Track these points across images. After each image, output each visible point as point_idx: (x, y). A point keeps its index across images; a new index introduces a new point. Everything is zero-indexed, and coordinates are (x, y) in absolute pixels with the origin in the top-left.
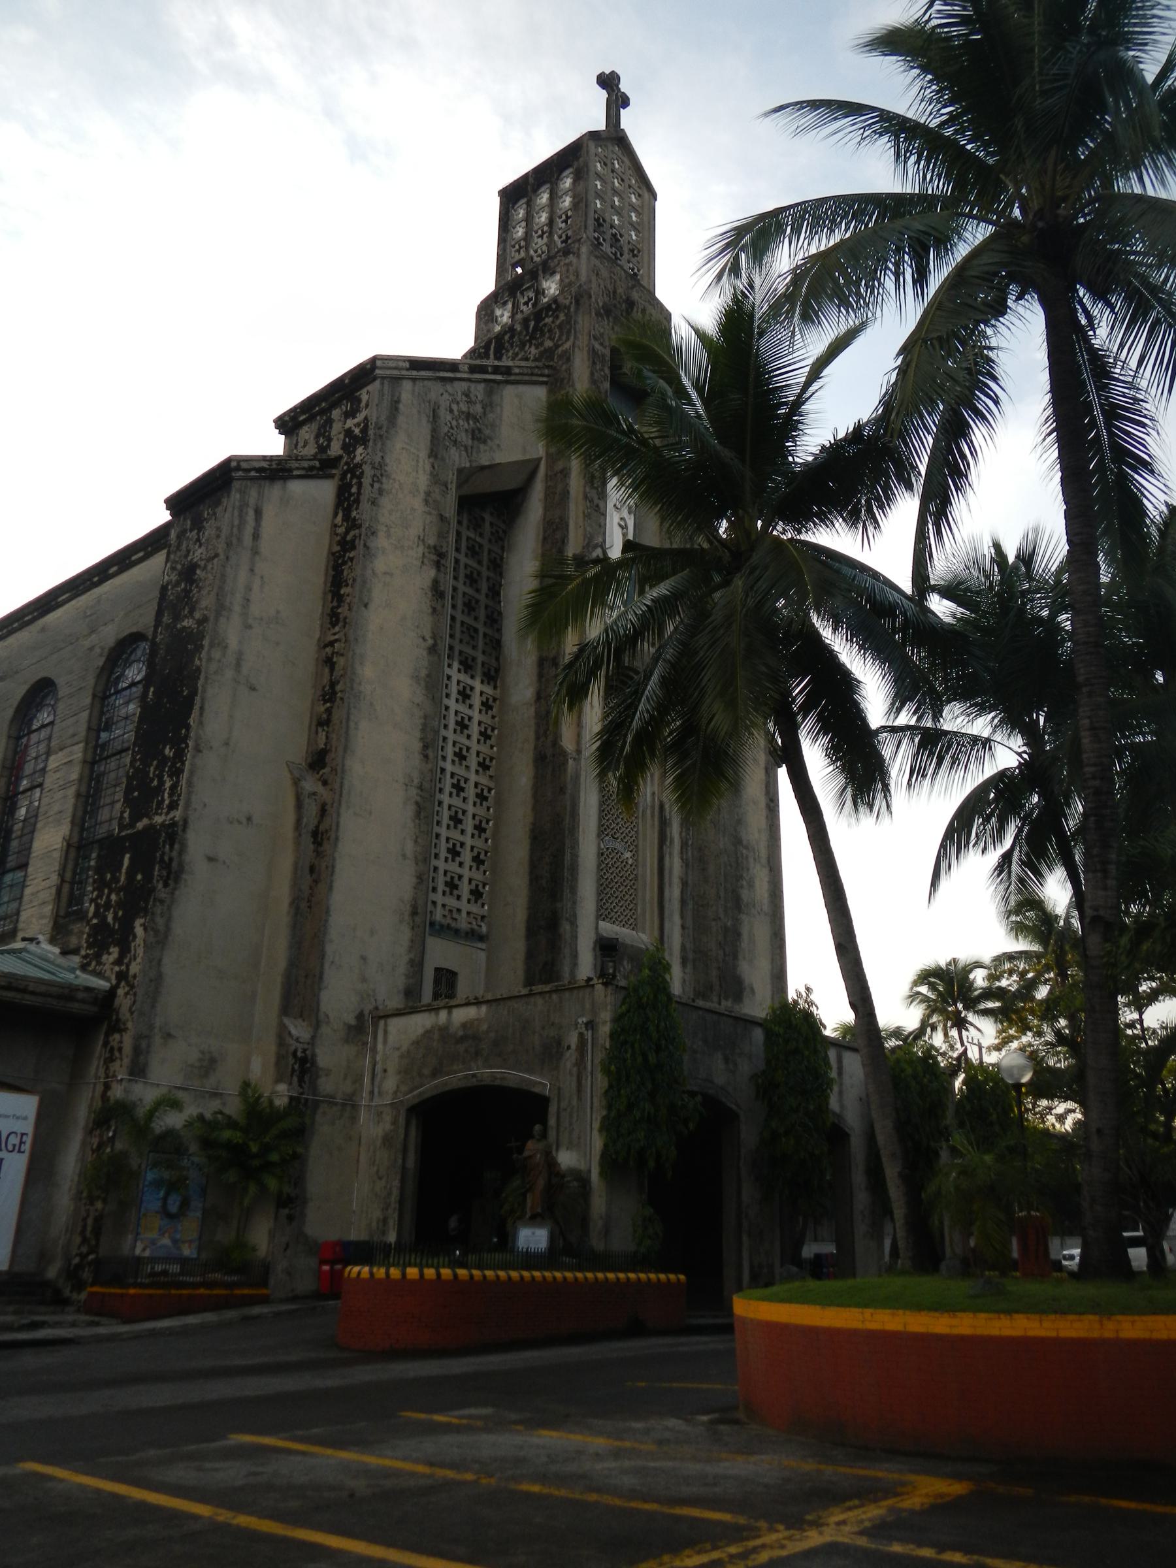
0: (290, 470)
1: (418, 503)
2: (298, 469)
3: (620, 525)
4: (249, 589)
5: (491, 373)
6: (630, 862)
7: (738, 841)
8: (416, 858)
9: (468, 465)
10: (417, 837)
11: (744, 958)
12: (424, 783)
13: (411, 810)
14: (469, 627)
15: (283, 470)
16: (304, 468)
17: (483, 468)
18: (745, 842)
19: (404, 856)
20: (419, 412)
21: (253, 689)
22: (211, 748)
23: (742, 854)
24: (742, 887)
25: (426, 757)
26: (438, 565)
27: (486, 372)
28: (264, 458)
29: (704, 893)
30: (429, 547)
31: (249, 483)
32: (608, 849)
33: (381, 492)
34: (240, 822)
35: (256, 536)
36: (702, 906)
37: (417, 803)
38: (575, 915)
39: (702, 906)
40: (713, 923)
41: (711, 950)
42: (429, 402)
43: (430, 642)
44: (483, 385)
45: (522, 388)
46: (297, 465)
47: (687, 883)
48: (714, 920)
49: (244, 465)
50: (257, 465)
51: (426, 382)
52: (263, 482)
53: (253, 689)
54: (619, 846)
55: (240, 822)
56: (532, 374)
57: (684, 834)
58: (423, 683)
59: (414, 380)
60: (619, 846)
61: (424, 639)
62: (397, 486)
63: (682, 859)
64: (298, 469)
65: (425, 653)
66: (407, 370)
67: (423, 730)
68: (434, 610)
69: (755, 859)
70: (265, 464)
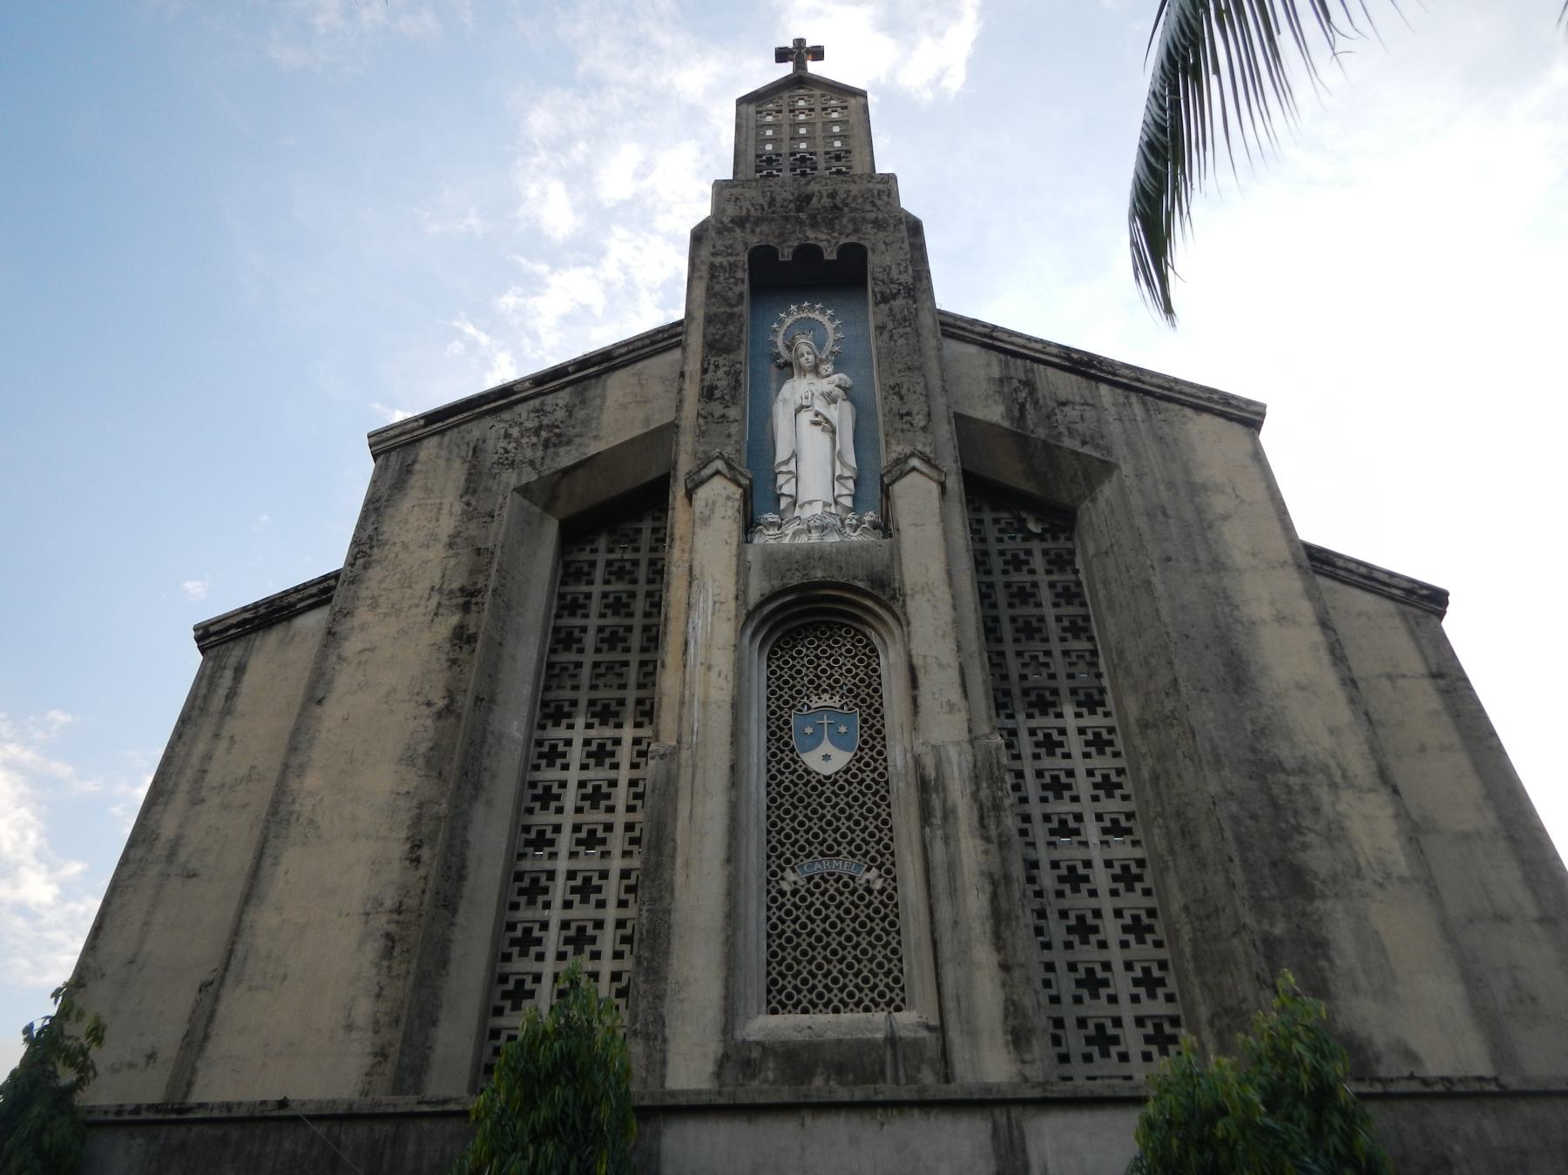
0: (294, 605)
1: (436, 553)
2: (301, 600)
3: (816, 423)
4: (208, 757)
5: (574, 373)
6: (878, 885)
7: (1264, 768)
8: (377, 1022)
9: (534, 477)
10: (381, 988)
11: (1355, 989)
12: (405, 900)
13: (374, 948)
14: (610, 666)
15: (282, 609)
16: (312, 596)
17: (567, 472)
18: (1290, 763)
19: (349, 1027)
20: (448, 460)
21: (191, 875)
22: (103, 975)
23: (1289, 789)
24: (1305, 847)
25: (416, 861)
26: (466, 608)
27: (568, 374)
28: (245, 609)
29: (1205, 889)
30: (451, 592)
31: (231, 644)
32: (810, 879)
33: (366, 567)
34: (131, 1066)
35: (232, 695)
36: (1208, 917)
37: (388, 936)
38: (660, 1021)
39: (1208, 917)
40: (1235, 942)
41: (1245, 1000)
42: (468, 444)
43: (441, 704)
44: (569, 390)
45: (640, 365)
46: (299, 596)
47: (1007, 878)
48: (1234, 934)
49: (213, 629)
50: (234, 621)
51: (463, 428)
52: (253, 636)
53: (191, 875)
54: (842, 866)
55: (131, 1066)
56: (653, 343)
57: (985, 792)
58: (420, 762)
59: (442, 432)
60: (842, 866)
61: (429, 704)
62: (398, 548)
63: (987, 839)
64: (301, 600)
65: (429, 722)
66: (425, 426)
67: (416, 822)
68: (454, 662)
69: (1334, 786)
70: (247, 615)
